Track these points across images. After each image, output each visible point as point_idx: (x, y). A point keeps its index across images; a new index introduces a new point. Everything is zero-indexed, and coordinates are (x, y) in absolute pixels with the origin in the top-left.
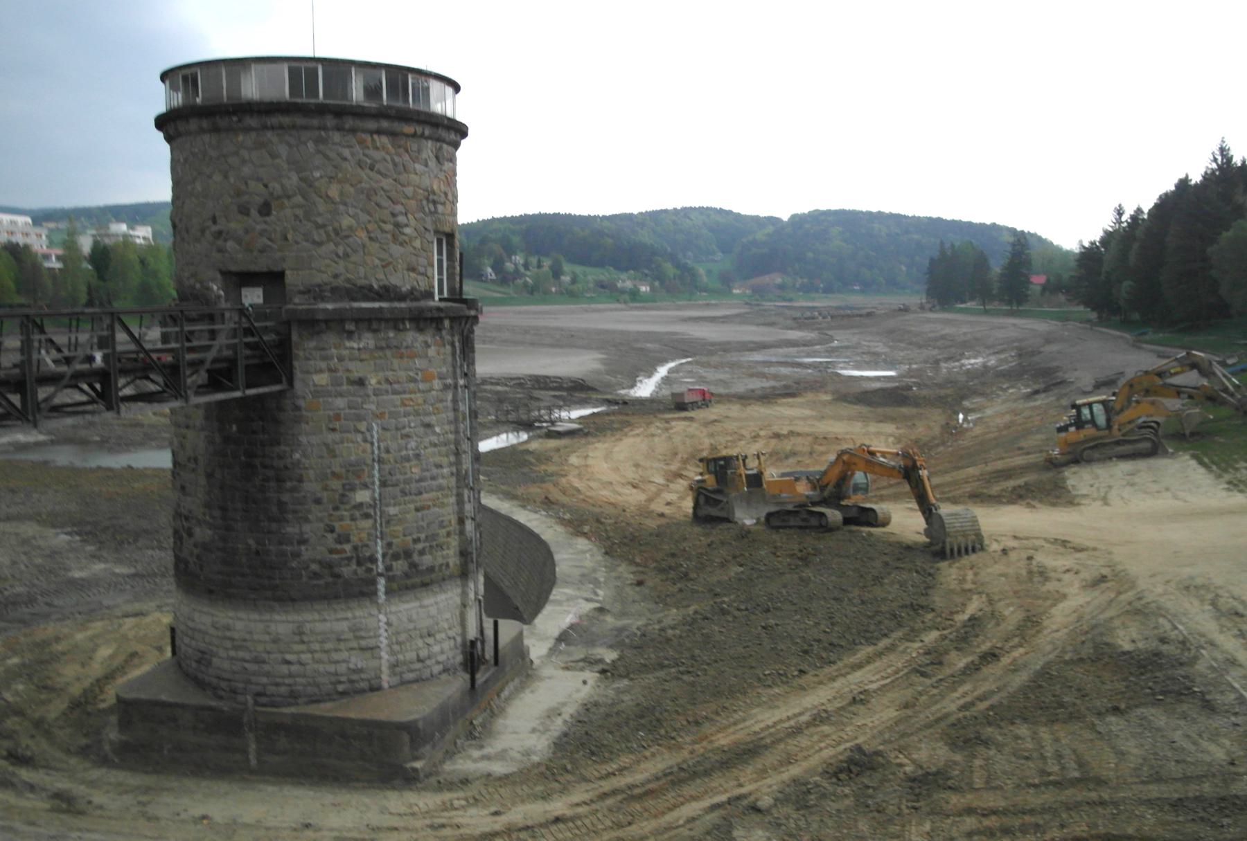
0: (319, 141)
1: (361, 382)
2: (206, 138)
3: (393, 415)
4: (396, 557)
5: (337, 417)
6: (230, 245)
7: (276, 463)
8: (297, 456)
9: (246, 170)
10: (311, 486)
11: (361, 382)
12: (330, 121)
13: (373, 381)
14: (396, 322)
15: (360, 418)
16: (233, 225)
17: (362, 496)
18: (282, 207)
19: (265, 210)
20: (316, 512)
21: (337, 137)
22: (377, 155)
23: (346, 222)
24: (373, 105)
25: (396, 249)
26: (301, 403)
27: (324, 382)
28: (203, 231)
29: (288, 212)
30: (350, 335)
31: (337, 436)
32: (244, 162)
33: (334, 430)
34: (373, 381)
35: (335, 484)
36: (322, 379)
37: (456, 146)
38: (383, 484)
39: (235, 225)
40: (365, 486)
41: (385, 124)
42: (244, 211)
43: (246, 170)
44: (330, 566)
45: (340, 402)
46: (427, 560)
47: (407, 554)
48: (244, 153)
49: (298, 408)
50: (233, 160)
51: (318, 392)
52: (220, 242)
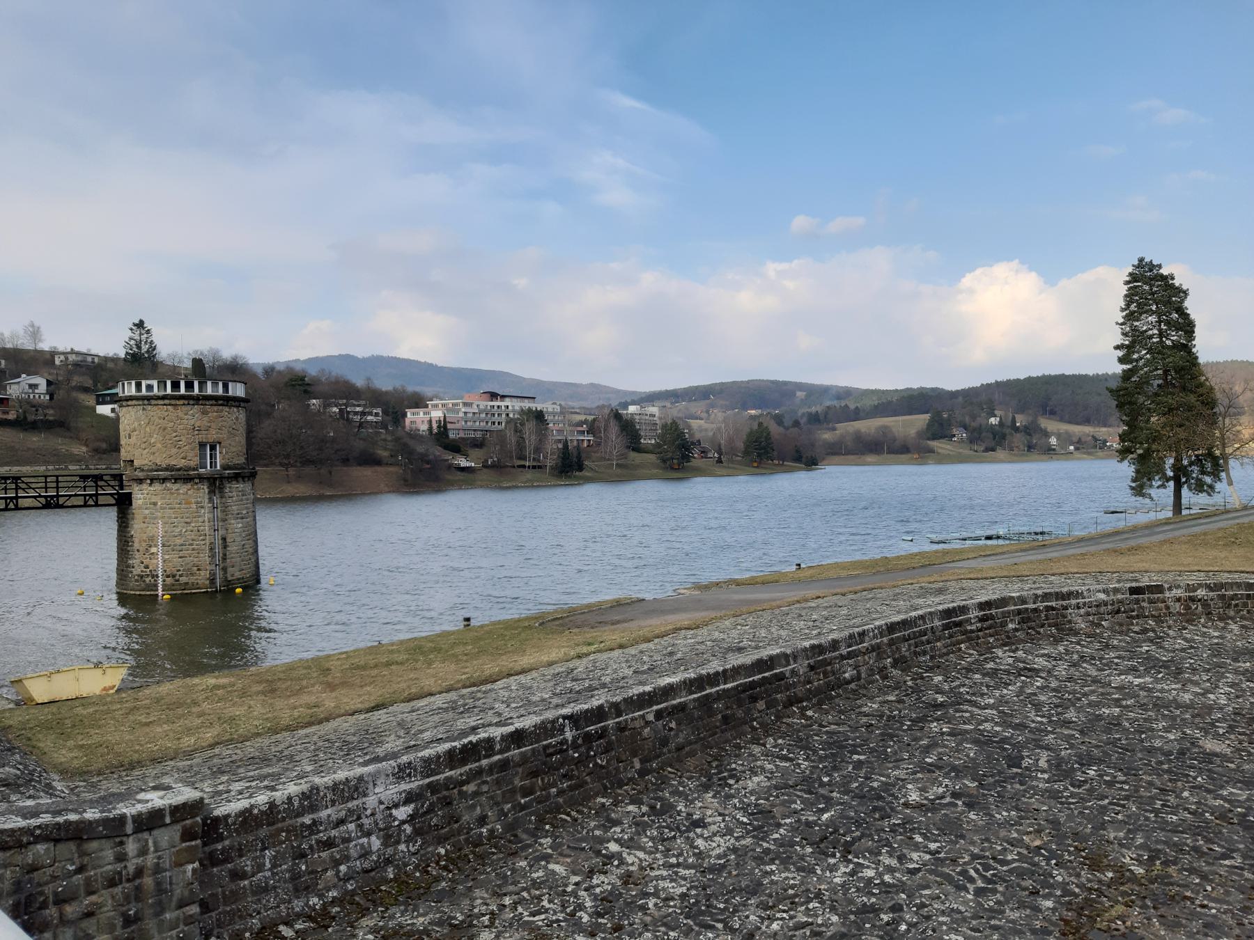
1: (155, 504)
4: (168, 576)
10: (136, 545)
11: (155, 504)
14: (164, 480)
17: (153, 550)
20: (137, 555)
25: (174, 451)
36: (140, 502)
38: (163, 545)
40: (156, 546)
41: (167, 402)
44: (142, 577)
45: (147, 512)
46: (183, 580)
47: (174, 576)
51: (140, 508)
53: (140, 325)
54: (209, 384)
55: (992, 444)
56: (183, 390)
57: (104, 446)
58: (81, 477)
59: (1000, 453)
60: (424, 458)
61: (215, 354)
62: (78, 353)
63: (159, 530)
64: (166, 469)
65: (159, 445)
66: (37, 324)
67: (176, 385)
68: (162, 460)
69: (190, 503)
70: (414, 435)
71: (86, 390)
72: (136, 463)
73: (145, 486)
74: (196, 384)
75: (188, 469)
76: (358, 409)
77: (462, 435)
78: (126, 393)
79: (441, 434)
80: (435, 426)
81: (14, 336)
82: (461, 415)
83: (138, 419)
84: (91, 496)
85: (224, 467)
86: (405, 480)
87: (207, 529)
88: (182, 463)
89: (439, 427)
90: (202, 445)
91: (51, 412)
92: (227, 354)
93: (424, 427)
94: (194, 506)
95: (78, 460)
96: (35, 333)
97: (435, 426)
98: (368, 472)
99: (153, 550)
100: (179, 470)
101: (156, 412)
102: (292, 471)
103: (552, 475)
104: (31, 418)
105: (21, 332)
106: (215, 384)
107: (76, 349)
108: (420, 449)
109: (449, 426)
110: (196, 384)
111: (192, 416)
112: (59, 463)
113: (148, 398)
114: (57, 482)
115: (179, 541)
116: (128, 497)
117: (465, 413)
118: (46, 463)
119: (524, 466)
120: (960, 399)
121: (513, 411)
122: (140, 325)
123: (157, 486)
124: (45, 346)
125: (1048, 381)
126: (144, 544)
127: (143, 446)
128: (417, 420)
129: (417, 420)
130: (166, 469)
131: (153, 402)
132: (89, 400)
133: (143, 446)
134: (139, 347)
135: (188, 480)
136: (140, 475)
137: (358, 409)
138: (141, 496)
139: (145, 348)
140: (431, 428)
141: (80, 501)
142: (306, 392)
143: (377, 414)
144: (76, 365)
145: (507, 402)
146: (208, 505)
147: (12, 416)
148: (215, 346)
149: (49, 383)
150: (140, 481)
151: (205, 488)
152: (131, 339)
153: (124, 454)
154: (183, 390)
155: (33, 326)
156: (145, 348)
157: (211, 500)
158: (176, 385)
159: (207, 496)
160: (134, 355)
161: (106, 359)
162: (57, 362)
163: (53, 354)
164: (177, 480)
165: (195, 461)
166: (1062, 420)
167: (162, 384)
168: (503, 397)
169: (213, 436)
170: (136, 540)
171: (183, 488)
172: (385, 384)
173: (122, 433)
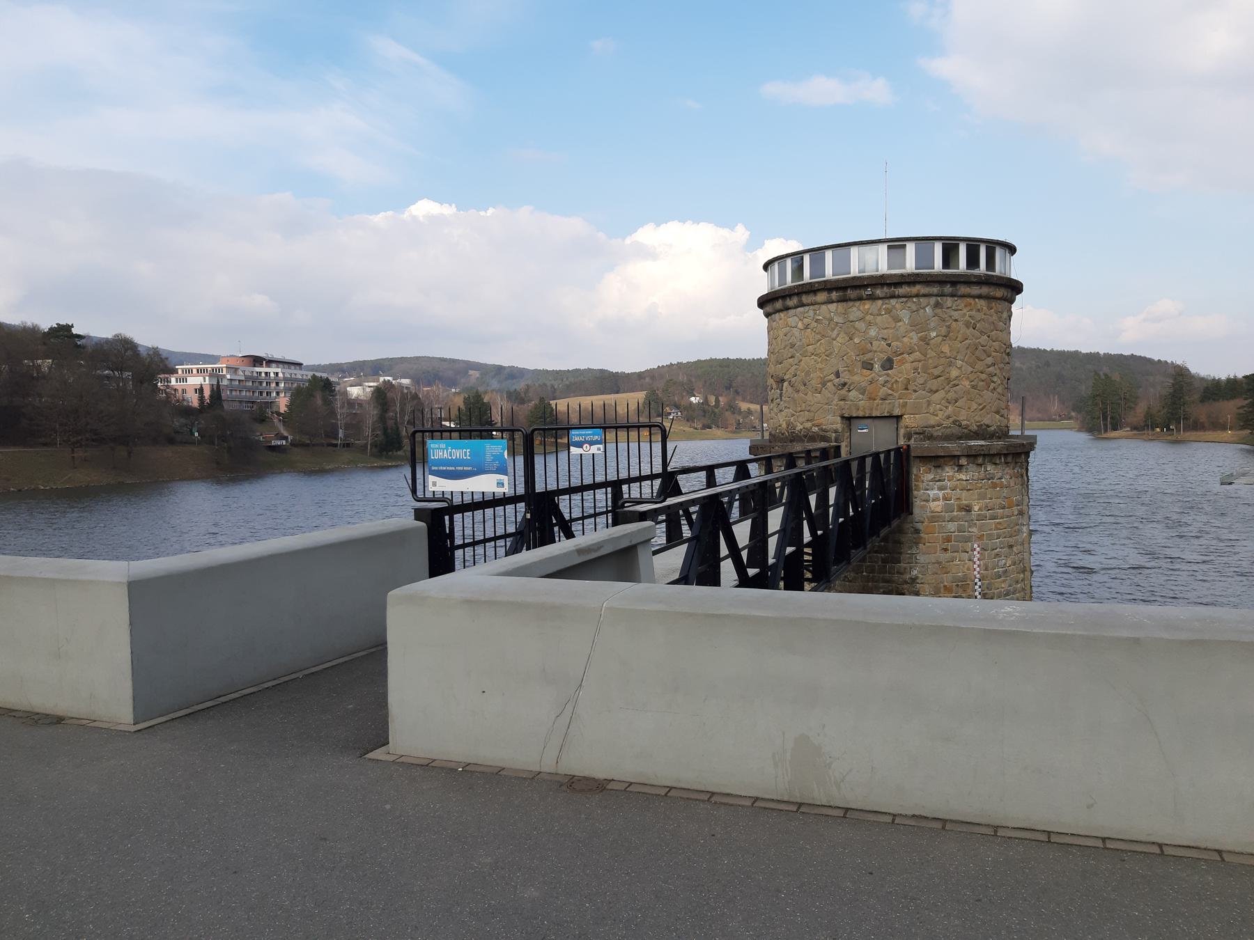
0: (937, 305)
2: (833, 307)
3: (990, 537)
5: (948, 540)
6: (853, 394)
7: (896, 577)
8: (915, 572)
9: (873, 333)
11: (968, 509)
12: (948, 289)
13: (976, 508)
15: (968, 540)
16: (856, 378)
18: (903, 362)
19: (888, 364)
21: (949, 301)
22: (979, 316)
23: (954, 373)
25: (987, 395)
26: (919, 526)
27: (939, 509)
28: (824, 384)
29: (908, 366)
30: (960, 467)
31: (949, 555)
32: (870, 324)
33: (946, 550)
34: (976, 508)
36: (937, 506)
37: (1012, 301)
39: (861, 377)
42: (868, 366)
43: (873, 333)
45: (952, 526)
48: (869, 318)
49: (917, 531)
50: (861, 326)
51: (934, 518)
52: (843, 392)
55: (707, 421)
59: (715, 431)
65: (967, 383)
68: (970, 416)
72: (908, 420)
73: (949, 471)
77: (236, 406)
86: (218, 463)
98: (168, 452)
102: (79, 453)
103: (372, 455)
119: (336, 445)
120: (647, 380)
121: (285, 380)
123: (969, 474)
125: (726, 363)
127: (933, 384)
130: (976, 435)
131: (963, 289)
133: (933, 384)
136: (953, 447)
140: (202, 398)
145: (272, 370)
150: (936, 461)
166: (744, 400)
168: (270, 362)
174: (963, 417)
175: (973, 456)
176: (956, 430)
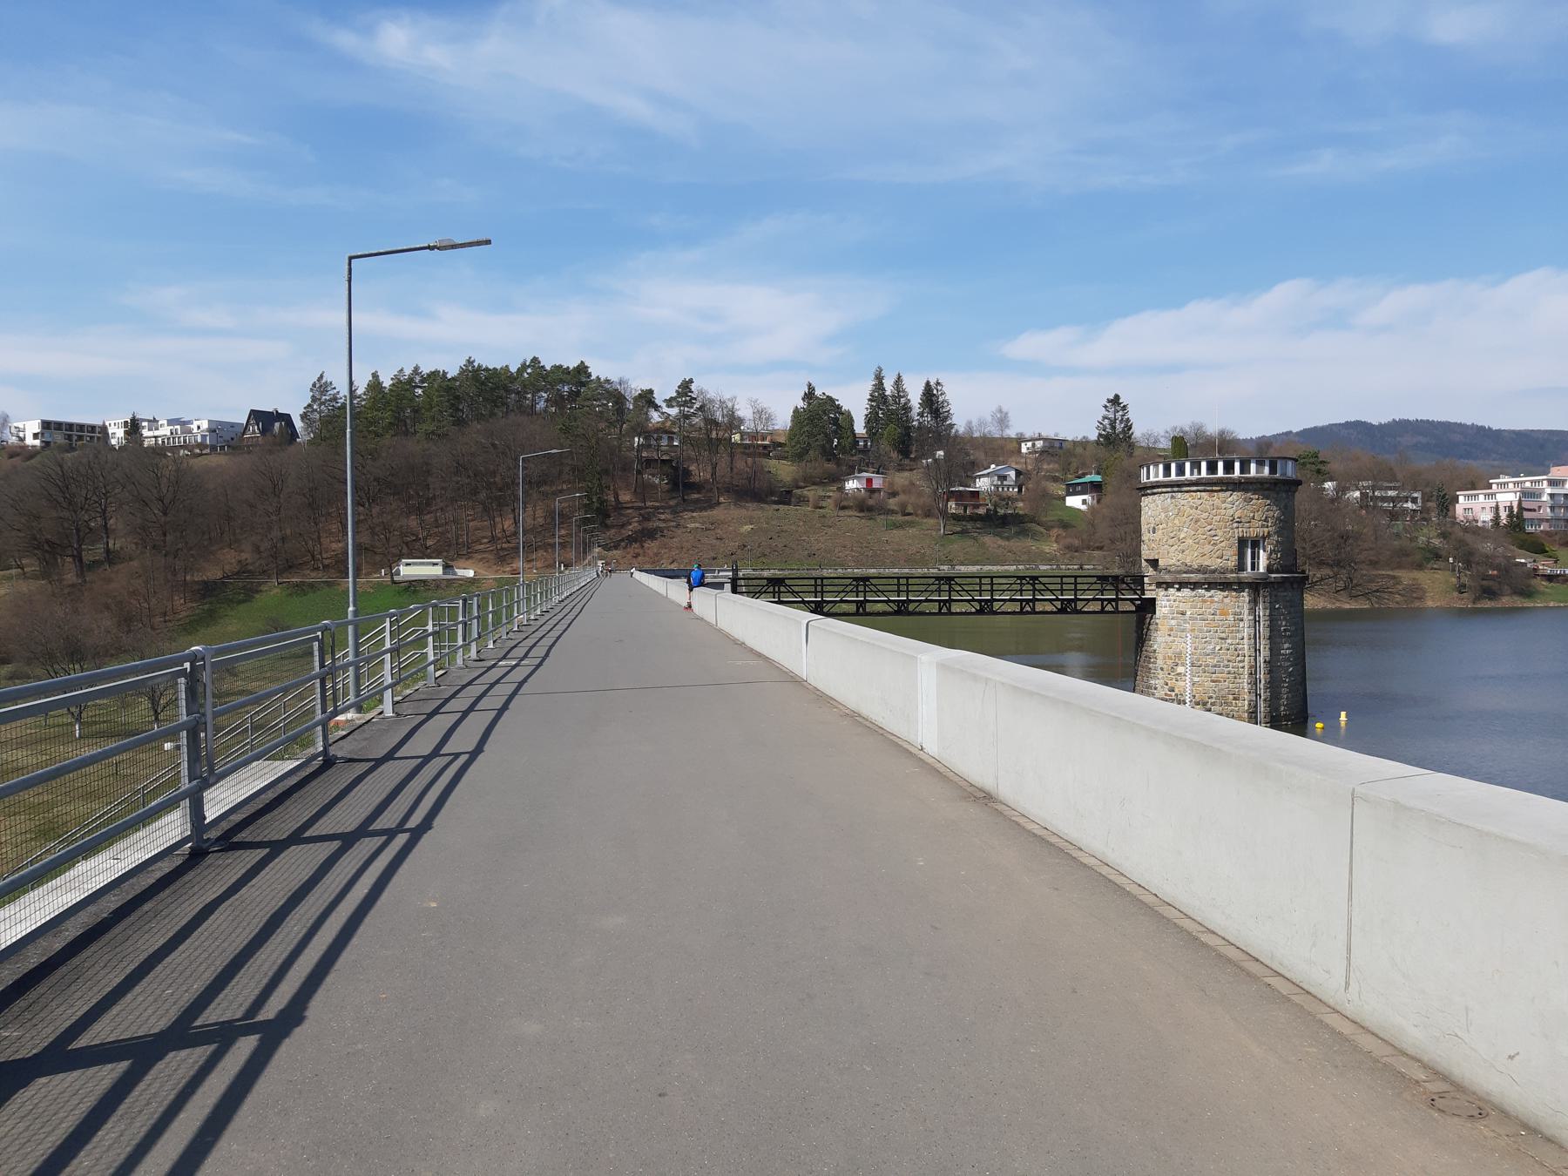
1: (1183, 614)
10: (1160, 662)
11: (1183, 614)
14: (1195, 586)
17: (1180, 669)
24: (1196, 476)
25: (1208, 548)
35: (1169, 662)
38: (1193, 665)
45: (1173, 622)
51: (1165, 617)
53: (1115, 401)
54: (1253, 466)
56: (1220, 472)
57: (1076, 542)
58: (1099, 578)
60: (1488, 561)
61: (1198, 431)
62: (1045, 440)
63: (1187, 645)
64: (1198, 571)
66: (1005, 409)
67: (1212, 468)
68: (1193, 559)
69: (1226, 614)
70: (1472, 528)
71: (1055, 479)
72: (1161, 563)
73: (1171, 591)
74: (1237, 465)
75: (1224, 571)
76: (1391, 493)
78: (1152, 479)
79: (1515, 525)
80: (1503, 515)
81: (982, 423)
82: (1545, 498)
83: (1165, 510)
84: (1110, 601)
85: (1269, 569)
87: (1246, 646)
88: (1215, 563)
89: (1510, 516)
90: (1242, 542)
91: (1021, 504)
92: (1212, 429)
93: (1486, 517)
94: (1231, 617)
95: (1049, 560)
96: (1003, 420)
97: (1503, 515)
99: (1180, 669)
100: (1214, 572)
101: (1185, 500)
104: (1001, 512)
105: (989, 419)
106: (1260, 463)
107: (1044, 434)
108: (1488, 547)
109: (1526, 515)
110: (1237, 465)
111: (1232, 504)
112: (1029, 561)
113: (1179, 485)
114: (1076, 584)
115: (1210, 661)
116: (1154, 600)
117: (1552, 496)
118: (1018, 562)
122: (1115, 401)
123: (1186, 592)
124: (1011, 433)
126: (1169, 662)
127: (1171, 542)
128: (1477, 507)
129: (1477, 507)
130: (1198, 571)
132: (1059, 489)
133: (1171, 542)
134: (1114, 428)
135: (1225, 586)
136: (1168, 578)
137: (1391, 493)
138: (1167, 603)
139: (1119, 427)
140: (1497, 517)
141: (1096, 607)
142: (1319, 471)
143: (1414, 500)
144: (1043, 452)
146: (1246, 616)
147: (982, 511)
148: (1198, 420)
149: (1018, 473)
150: (1168, 585)
151: (1245, 596)
152: (1105, 418)
153: (1146, 553)
154: (1220, 472)
155: (1000, 411)
156: (1119, 427)
157: (1253, 611)
158: (1212, 468)
159: (1246, 606)
160: (1107, 437)
161: (1074, 442)
162: (1024, 450)
163: (1020, 440)
164: (1211, 586)
165: (1232, 563)
167: (1196, 465)
169: (1255, 531)
170: (1160, 657)
171: (1218, 595)
172: (1423, 463)
173: (1144, 528)
174: (1188, 561)
175: (1182, 585)
176: (1183, 568)
